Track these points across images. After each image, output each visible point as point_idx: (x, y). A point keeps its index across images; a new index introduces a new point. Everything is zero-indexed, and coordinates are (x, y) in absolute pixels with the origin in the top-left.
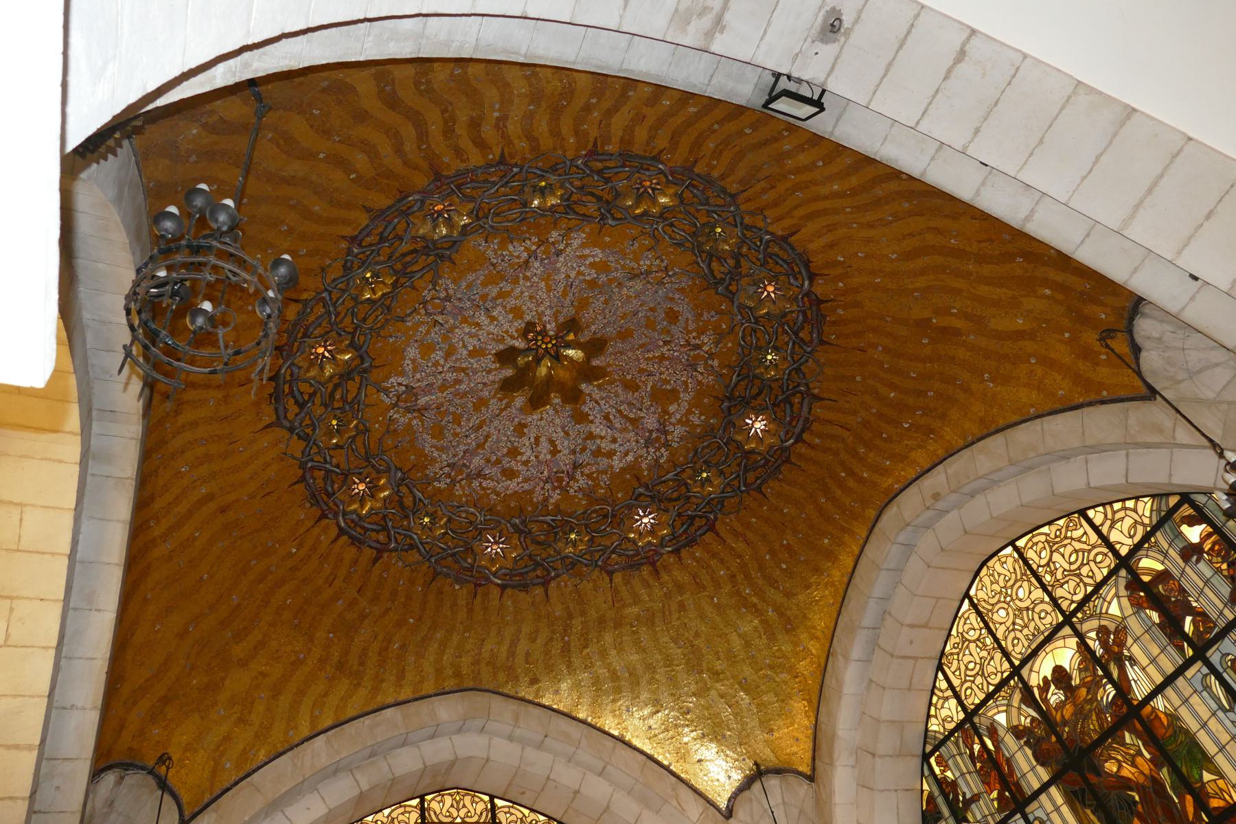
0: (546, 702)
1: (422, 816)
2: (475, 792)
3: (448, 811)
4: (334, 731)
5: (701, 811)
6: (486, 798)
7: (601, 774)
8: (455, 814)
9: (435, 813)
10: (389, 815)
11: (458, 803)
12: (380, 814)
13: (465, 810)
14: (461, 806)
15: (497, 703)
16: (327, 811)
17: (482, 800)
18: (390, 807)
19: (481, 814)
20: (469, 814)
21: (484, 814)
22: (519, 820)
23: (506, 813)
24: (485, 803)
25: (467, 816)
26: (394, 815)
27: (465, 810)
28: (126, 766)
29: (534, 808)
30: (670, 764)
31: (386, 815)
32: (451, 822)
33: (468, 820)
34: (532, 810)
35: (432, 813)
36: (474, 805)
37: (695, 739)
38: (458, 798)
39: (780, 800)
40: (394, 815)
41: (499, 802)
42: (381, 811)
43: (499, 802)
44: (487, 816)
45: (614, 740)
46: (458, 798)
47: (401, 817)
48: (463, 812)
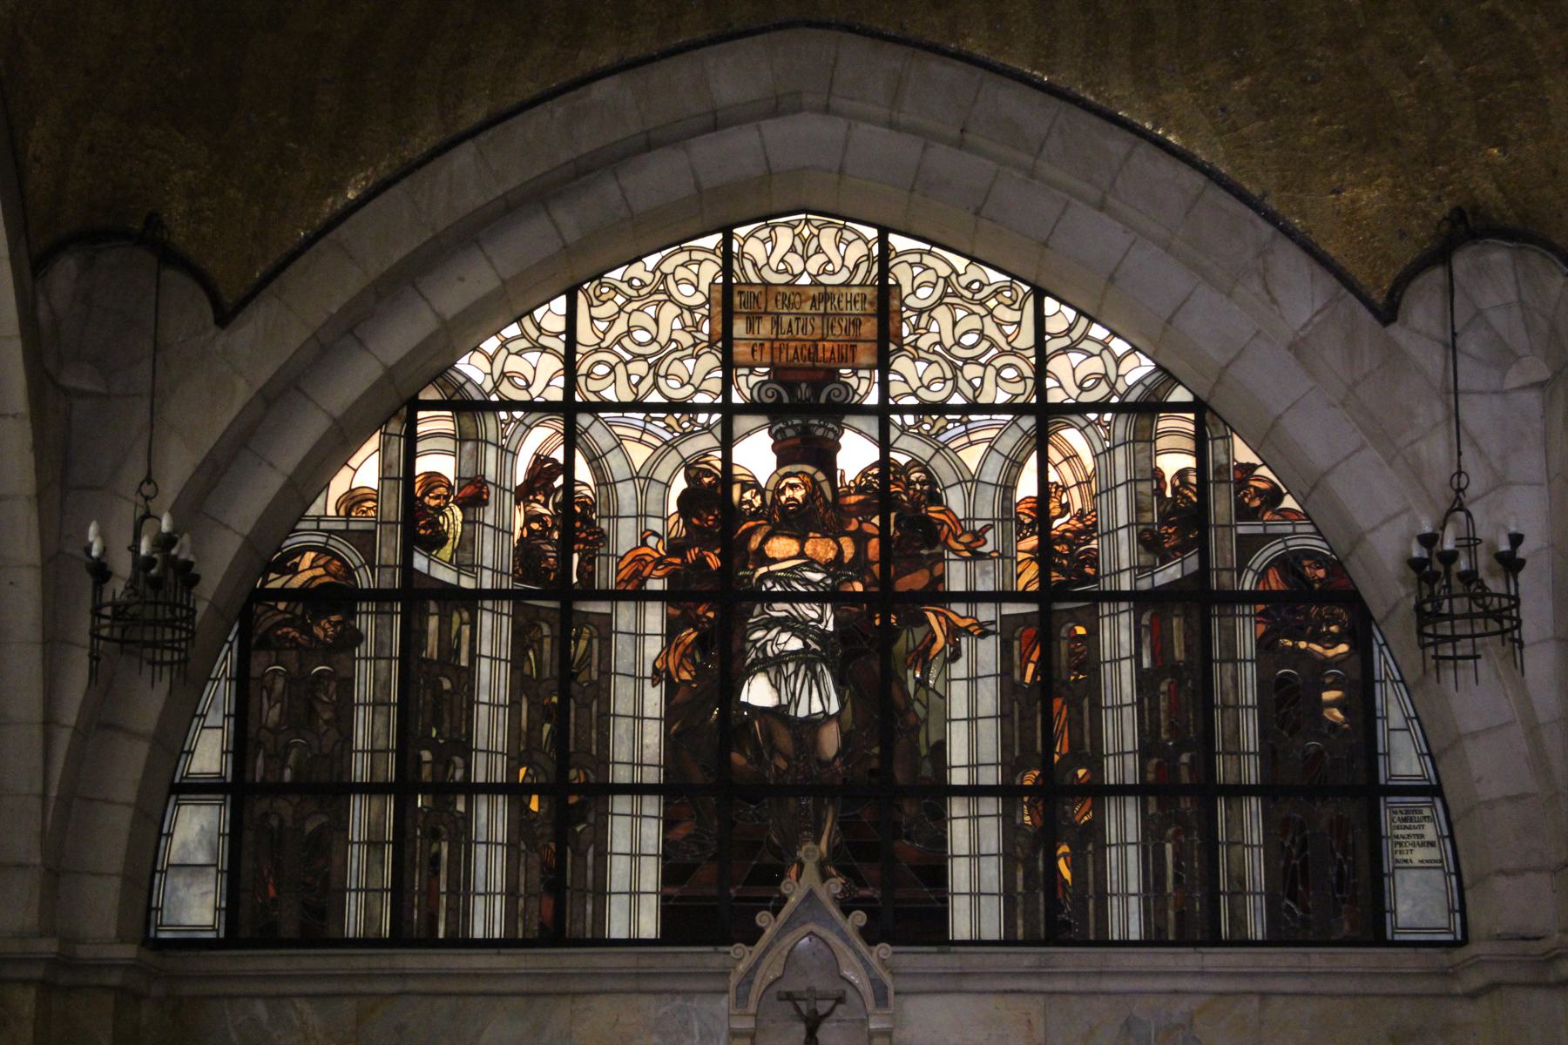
0: (972, 45)
1: (727, 270)
2: (846, 219)
3: (782, 260)
4: (490, 133)
5: (1318, 305)
6: (871, 233)
7: (1101, 207)
8: (796, 263)
9: (755, 264)
10: (658, 267)
11: (805, 243)
12: (636, 270)
13: (821, 259)
14: (811, 250)
15: (854, 50)
16: (496, 283)
17: (860, 236)
18: (660, 250)
19: (857, 266)
20: (830, 267)
21: (863, 268)
22: (941, 282)
23: (912, 265)
24: (867, 242)
25: (825, 272)
26: (667, 267)
27: (821, 259)
28: (91, 238)
29: (977, 254)
30: (1265, 195)
31: (650, 268)
32: (787, 284)
33: (824, 279)
34: (973, 260)
35: (748, 265)
36: (842, 247)
37: (1332, 142)
38: (806, 233)
39: (1513, 297)
40: (667, 267)
41: (898, 242)
42: (639, 259)
43: (898, 242)
44: (869, 271)
45: (1133, 137)
46: (806, 233)
47: (681, 273)
48: (814, 264)
